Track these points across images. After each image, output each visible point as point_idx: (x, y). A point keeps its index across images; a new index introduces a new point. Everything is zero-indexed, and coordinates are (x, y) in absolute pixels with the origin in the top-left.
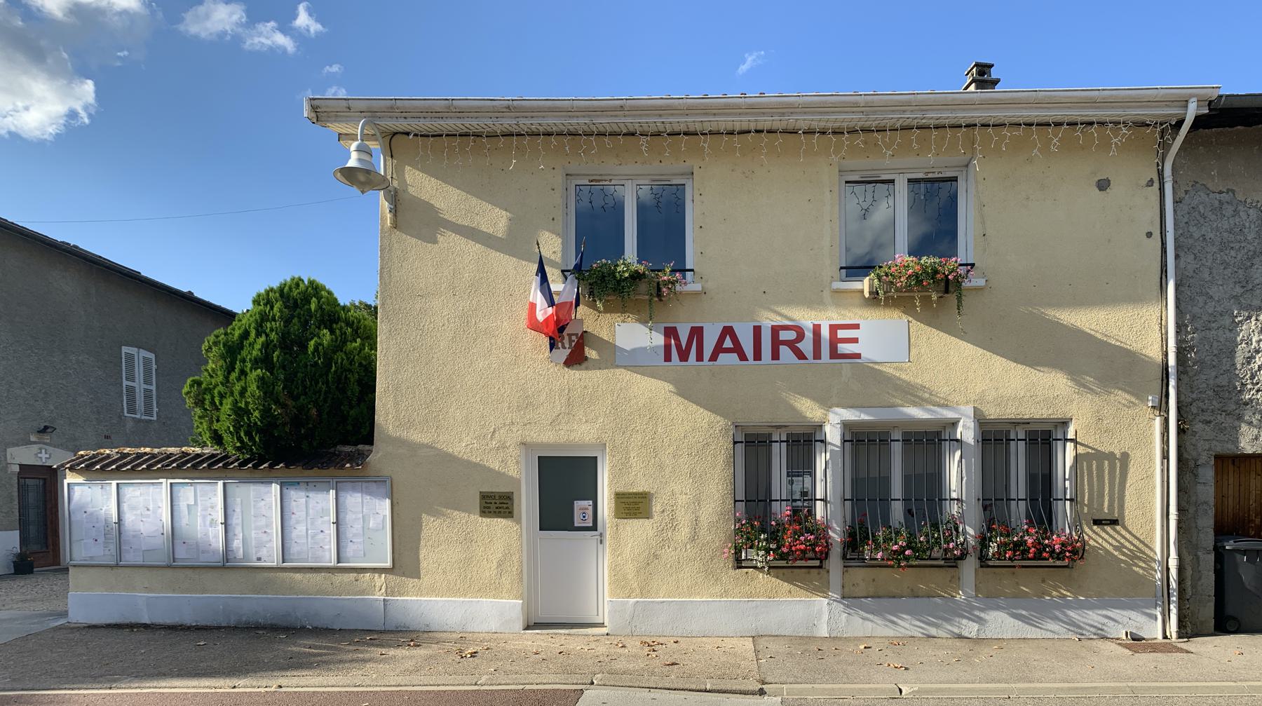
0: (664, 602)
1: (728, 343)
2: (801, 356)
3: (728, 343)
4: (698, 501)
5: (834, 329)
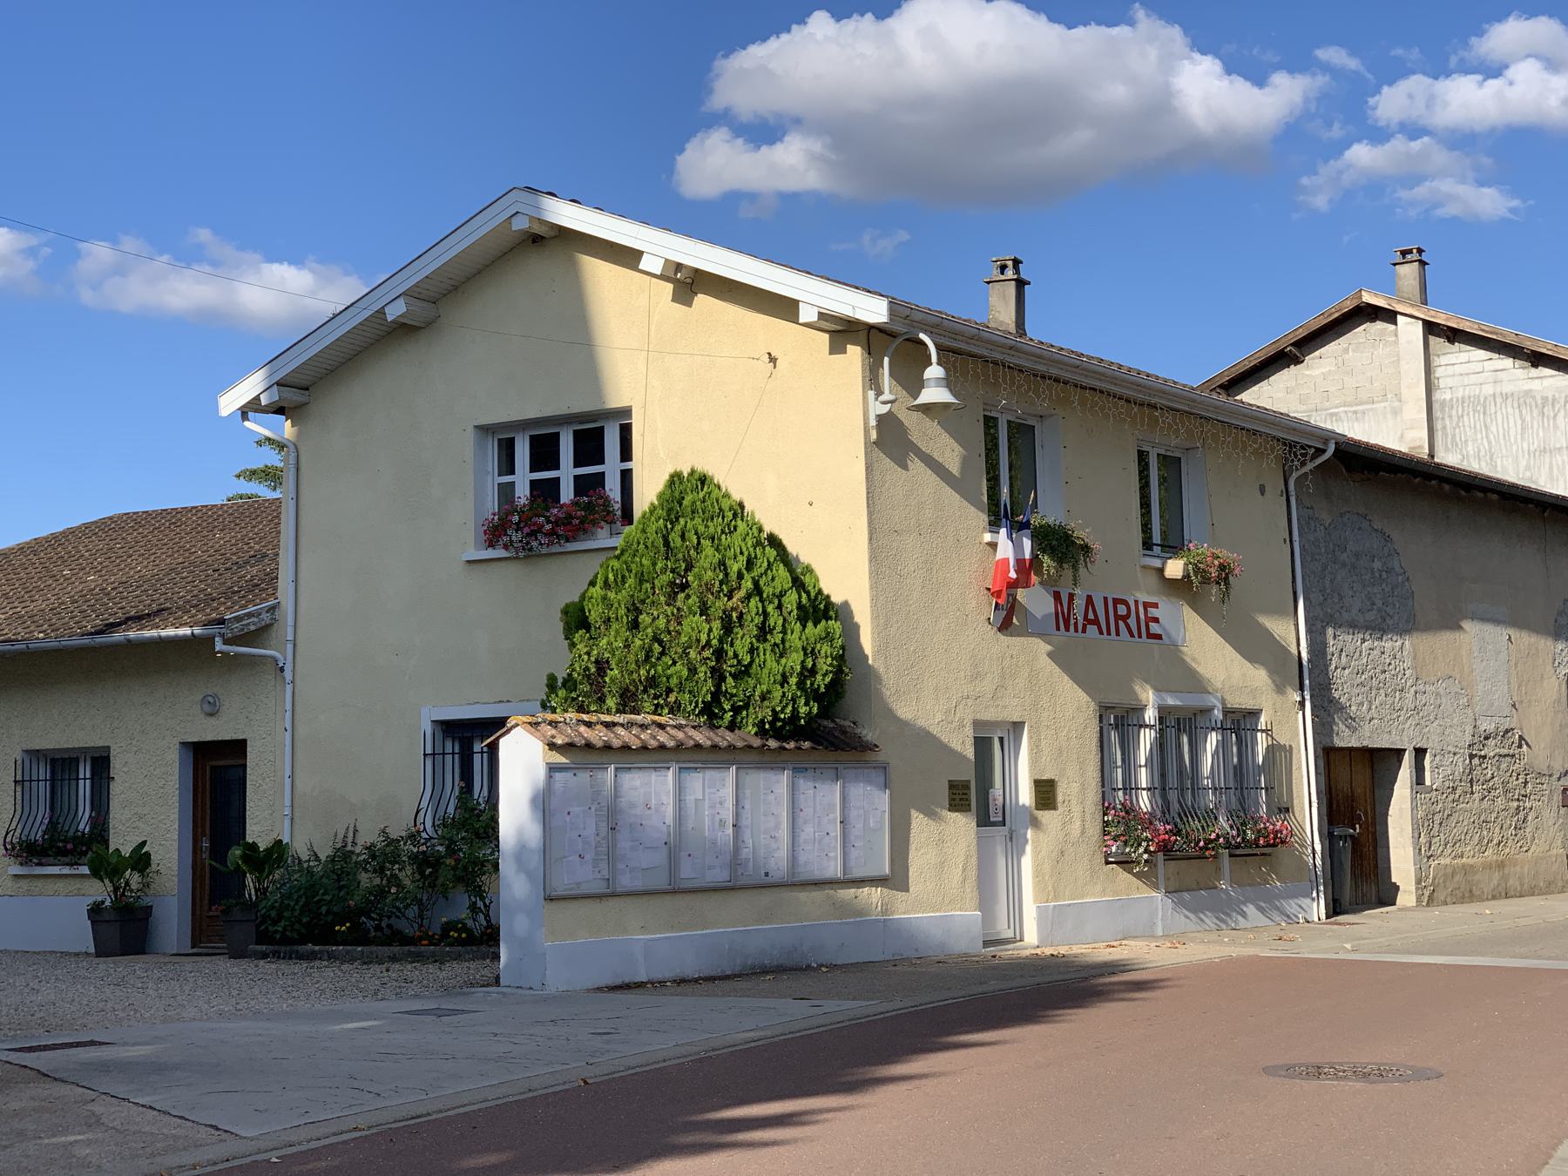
0: (1070, 905)
1: (1091, 616)
2: (1132, 635)
3: (1091, 616)
4: (1083, 788)
5: (1146, 605)
